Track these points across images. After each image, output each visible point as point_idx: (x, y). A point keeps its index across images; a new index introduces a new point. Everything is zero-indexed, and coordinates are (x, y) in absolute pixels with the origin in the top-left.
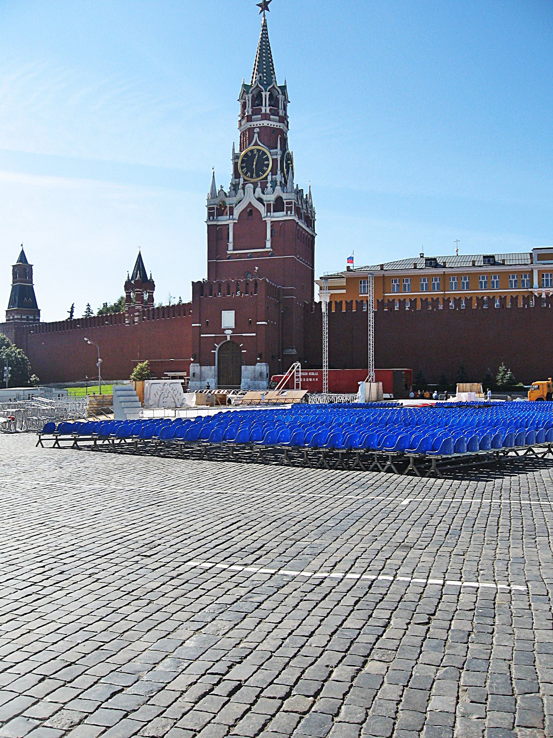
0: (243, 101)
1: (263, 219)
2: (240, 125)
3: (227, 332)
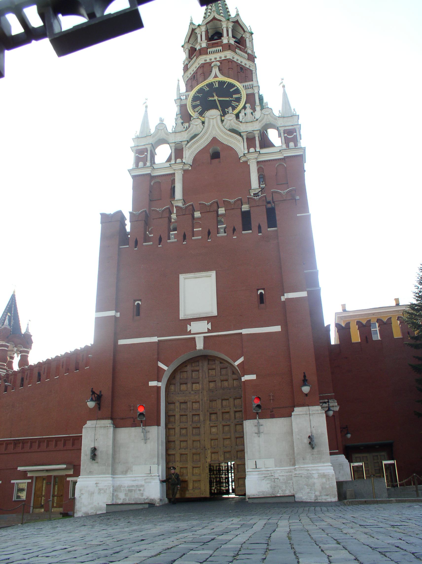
0: (190, 46)
1: (243, 159)
2: (186, 69)
3: (194, 327)
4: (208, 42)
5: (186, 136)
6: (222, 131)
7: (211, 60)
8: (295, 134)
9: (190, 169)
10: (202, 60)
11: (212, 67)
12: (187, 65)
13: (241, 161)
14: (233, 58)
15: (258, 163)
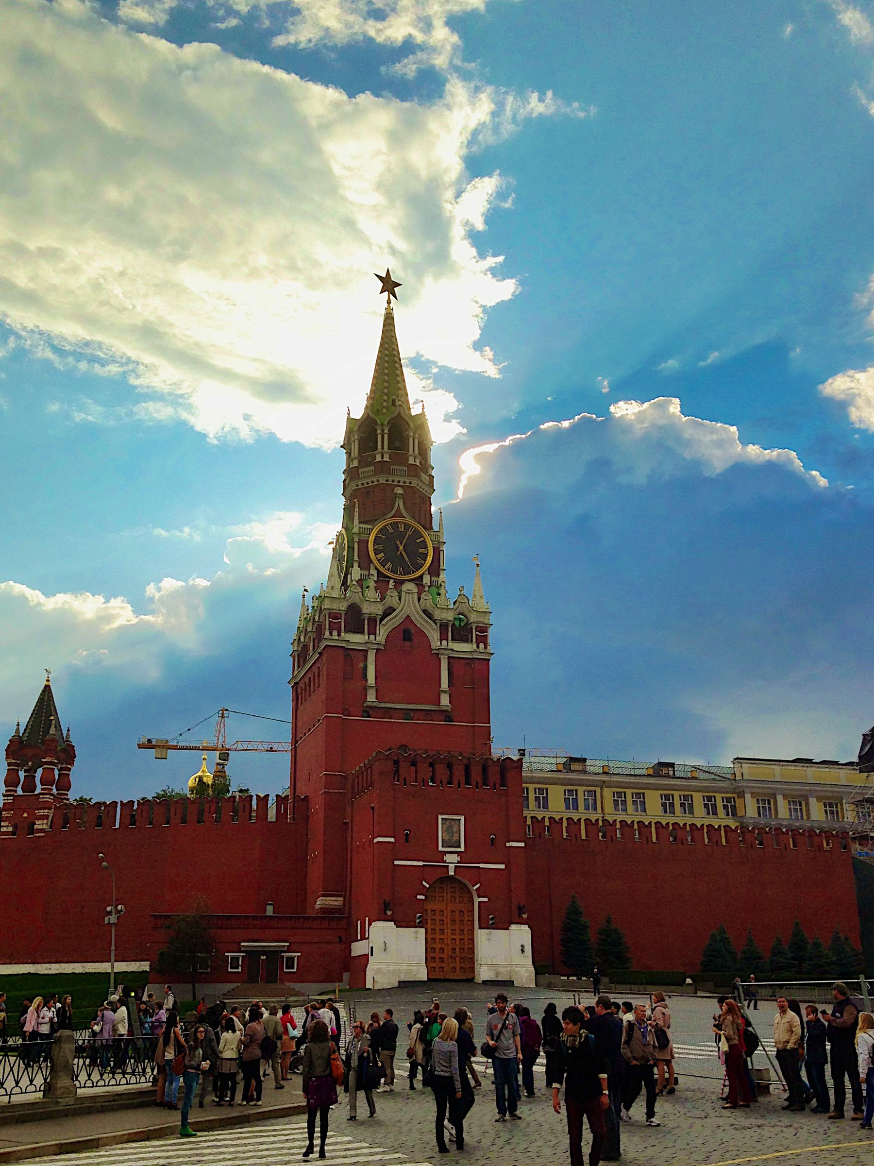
3: (448, 858)
6: (417, 612)
15: (449, 657)
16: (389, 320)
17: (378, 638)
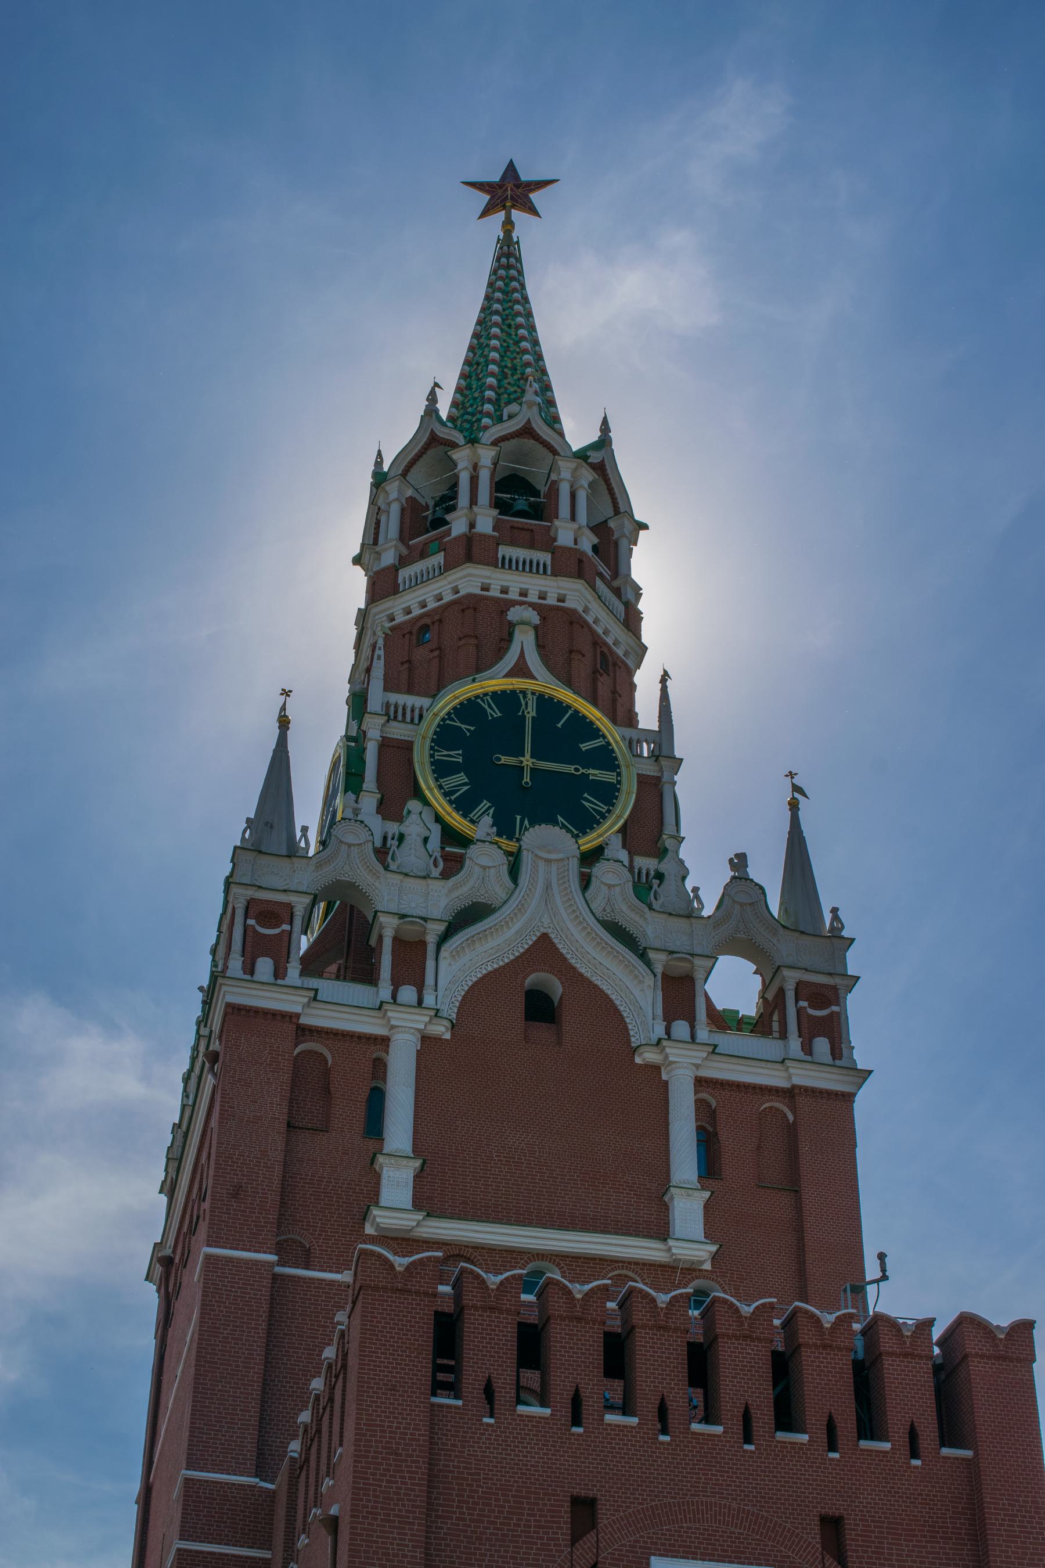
0: (409, 493)
4: (500, 514)
5: (443, 903)
7: (505, 591)
8: (835, 1008)
9: (448, 1036)
10: (471, 579)
11: (512, 626)
12: (395, 569)
13: (638, 1060)
14: (586, 610)
15: (700, 1083)
16: (508, 263)
17: (429, 1000)
